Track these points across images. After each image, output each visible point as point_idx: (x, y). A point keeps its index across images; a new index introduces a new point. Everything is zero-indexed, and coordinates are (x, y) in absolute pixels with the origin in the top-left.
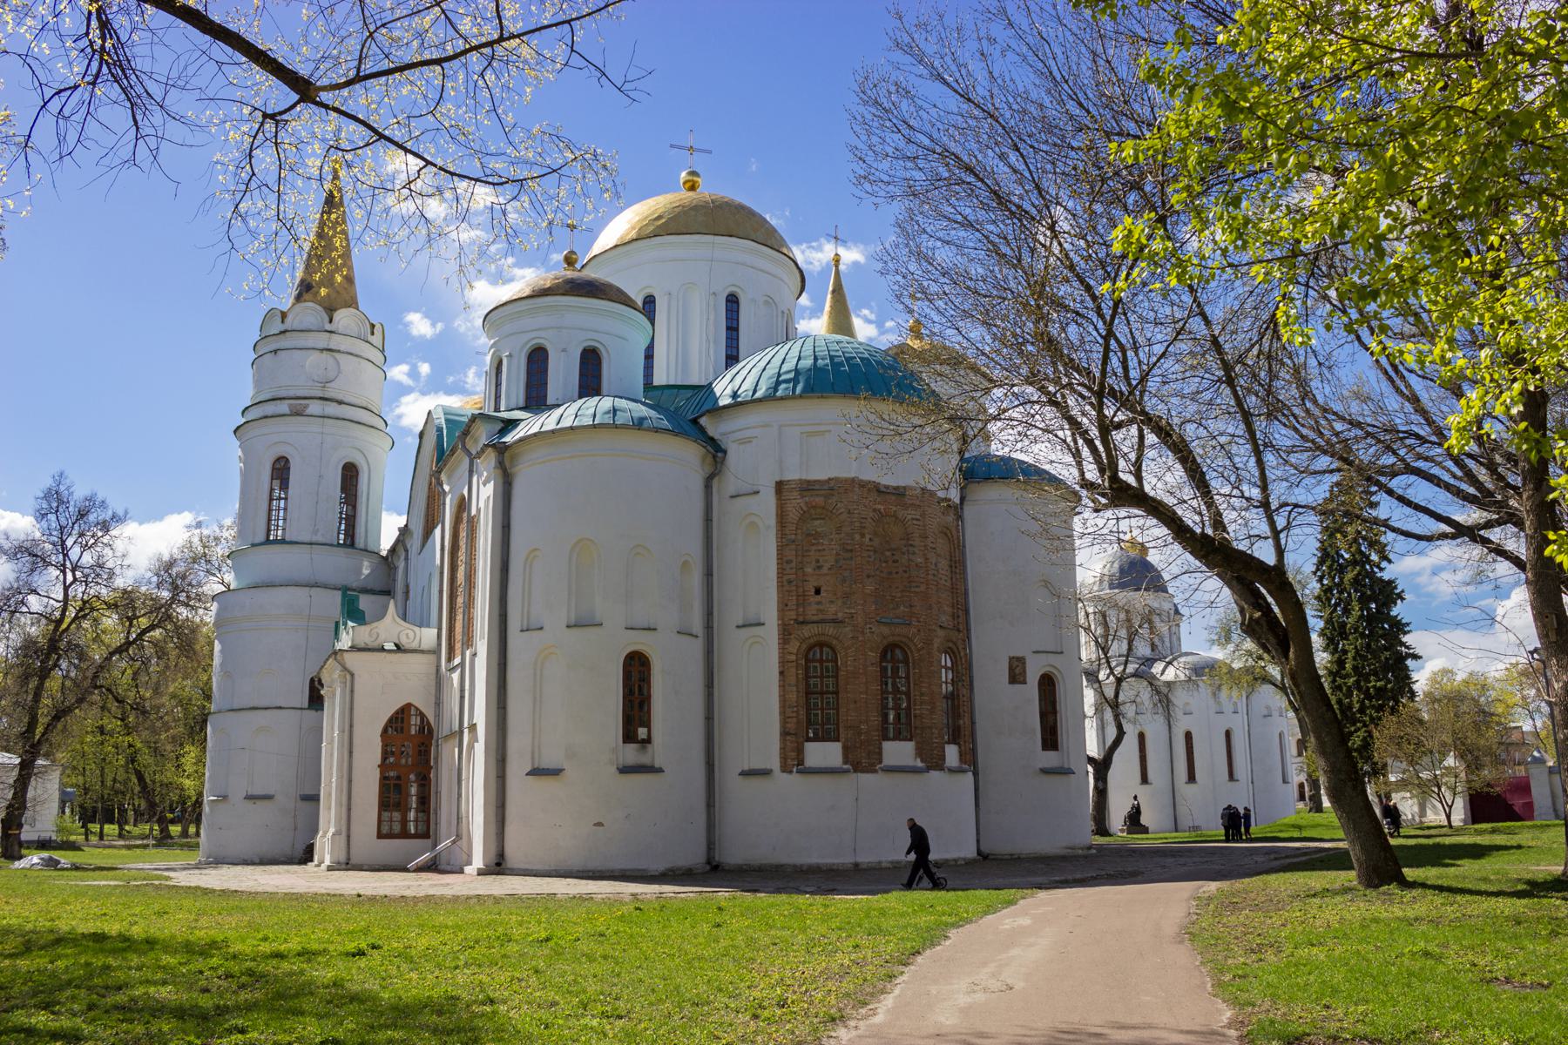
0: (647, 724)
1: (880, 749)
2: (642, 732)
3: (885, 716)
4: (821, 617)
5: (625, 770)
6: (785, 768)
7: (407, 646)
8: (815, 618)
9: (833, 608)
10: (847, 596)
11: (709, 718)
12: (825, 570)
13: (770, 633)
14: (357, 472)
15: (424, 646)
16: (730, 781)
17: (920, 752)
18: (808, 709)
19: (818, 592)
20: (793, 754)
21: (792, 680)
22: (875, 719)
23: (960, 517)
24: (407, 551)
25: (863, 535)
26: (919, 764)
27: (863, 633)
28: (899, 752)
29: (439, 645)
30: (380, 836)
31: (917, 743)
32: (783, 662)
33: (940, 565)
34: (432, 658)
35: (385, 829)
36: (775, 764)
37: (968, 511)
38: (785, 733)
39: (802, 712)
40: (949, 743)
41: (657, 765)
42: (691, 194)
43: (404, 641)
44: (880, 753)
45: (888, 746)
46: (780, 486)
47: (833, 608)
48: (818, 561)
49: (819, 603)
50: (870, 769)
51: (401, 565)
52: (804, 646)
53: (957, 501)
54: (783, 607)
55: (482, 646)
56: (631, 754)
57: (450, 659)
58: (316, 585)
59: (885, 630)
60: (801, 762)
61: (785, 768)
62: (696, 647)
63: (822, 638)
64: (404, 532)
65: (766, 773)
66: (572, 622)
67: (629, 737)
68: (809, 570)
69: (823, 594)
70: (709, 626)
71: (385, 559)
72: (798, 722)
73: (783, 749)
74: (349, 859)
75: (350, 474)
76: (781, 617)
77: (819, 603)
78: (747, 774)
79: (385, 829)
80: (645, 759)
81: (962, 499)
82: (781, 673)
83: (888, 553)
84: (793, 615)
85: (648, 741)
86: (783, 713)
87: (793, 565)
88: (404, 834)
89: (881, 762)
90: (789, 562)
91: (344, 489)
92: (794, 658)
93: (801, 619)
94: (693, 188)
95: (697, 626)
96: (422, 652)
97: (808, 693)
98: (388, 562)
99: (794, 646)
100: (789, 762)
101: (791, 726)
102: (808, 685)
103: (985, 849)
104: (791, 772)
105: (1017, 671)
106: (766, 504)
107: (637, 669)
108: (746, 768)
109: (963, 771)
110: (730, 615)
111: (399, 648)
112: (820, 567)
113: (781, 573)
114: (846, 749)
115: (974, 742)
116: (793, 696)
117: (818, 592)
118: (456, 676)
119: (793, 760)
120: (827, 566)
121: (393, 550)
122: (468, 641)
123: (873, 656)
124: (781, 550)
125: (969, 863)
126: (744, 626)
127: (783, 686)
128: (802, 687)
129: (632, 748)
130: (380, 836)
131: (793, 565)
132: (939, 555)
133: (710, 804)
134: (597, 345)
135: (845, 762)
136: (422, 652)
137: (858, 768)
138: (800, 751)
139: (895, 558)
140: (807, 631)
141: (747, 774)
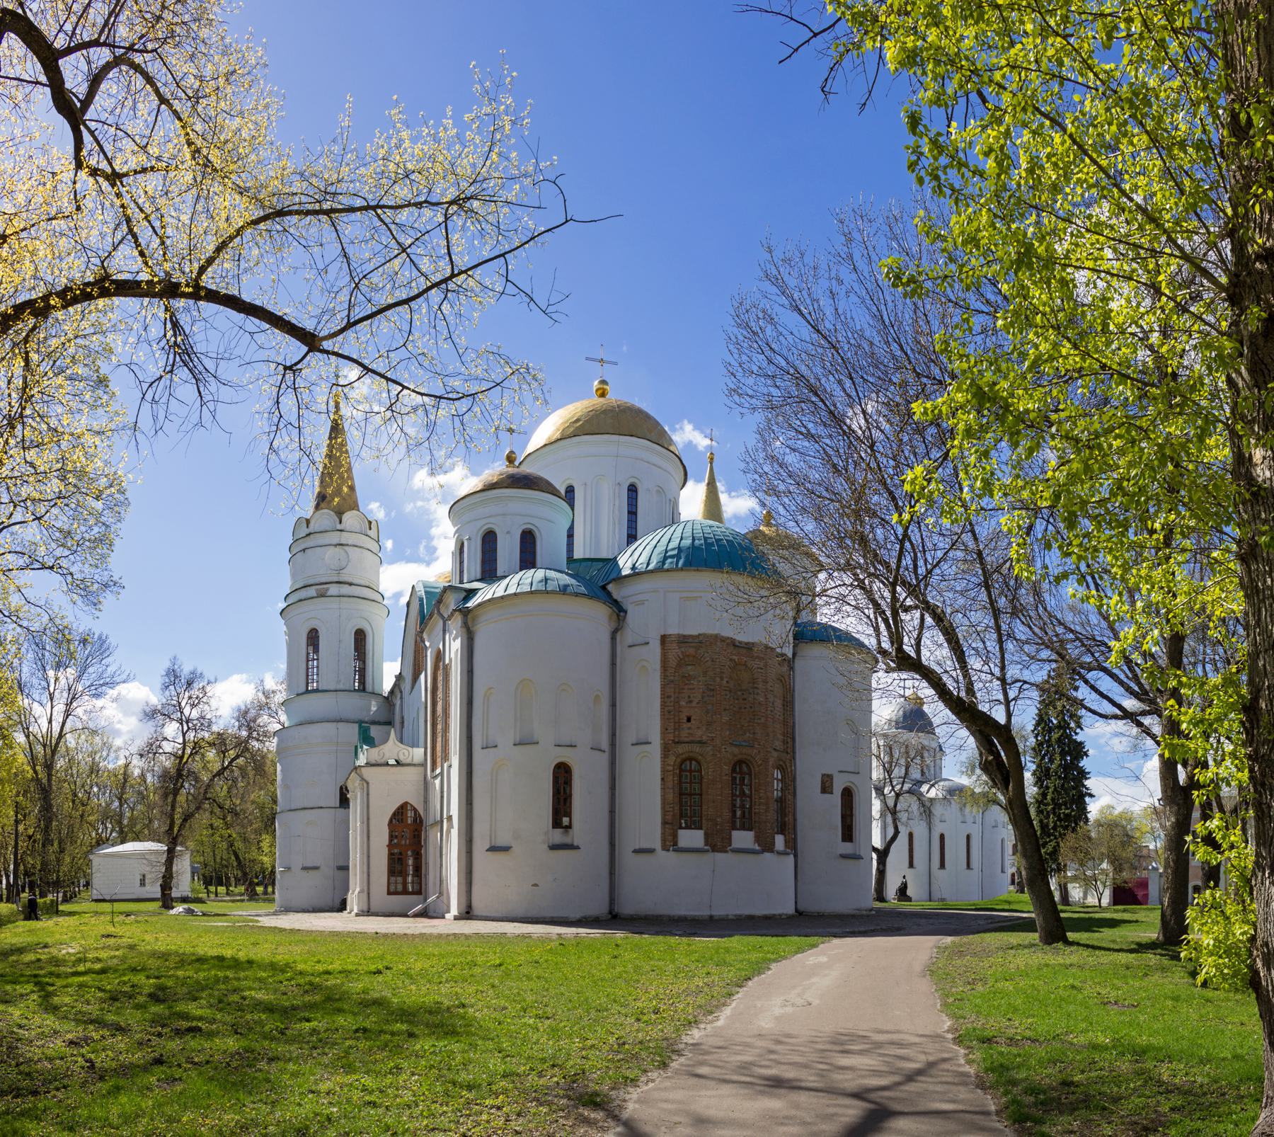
0: (569, 815)
1: (730, 836)
2: (565, 821)
3: (734, 812)
4: (691, 738)
5: (554, 847)
6: (665, 848)
7: (404, 762)
8: (687, 740)
9: (699, 733)
10: (709, 724)
11: (612, 812)
12: (694, 704)
13: (655, 749)
15: (415, 761)
18: (681, 806)
19: (689, 720)
20: (670, 838)
21: (670, 784)
22: (727, 814)
23: (792, 668)
24: (401, 692)
25: (722, 679)
26: (757, 848)
27: (720, 751)
28: (743, 838)
29: (426, 760)
32: (664, 771)
33: (776, 704)
34: (421, 769)
36: (657, 844)
37: (798, 664)
38: (664, 823)
39: (677, 808)
40: (778, 833)
41: (575, 844)
43: (402, 758)
44: (730, 839)
45: (735, 834)
47: (699, 733)
49: (689, 728)
50: (723, 850)
51: (398, 703)
52: (679, 760)
53: (790, 655)
54: (664, 731)
55: (455, 760)
56: (558, 836)
57: (433, 770)
59: (736, 750)
60: (675, 844)
61: (665, 848)
62: (604, 759)
63: (691, 754)
64: (399, 678)
65: (650, 851)
66: (517, 742)
67: (557, 824)
68: (683, 703)
69: (693, 722)
70: (613, 744)
71: (386, 698)
72: (674, 815)
73: (663, 834)
75: (360, 638)
76: (663, 738)
77: (689, 728)
78: (638, 851)
80: (567, 840)
81: (794, 655)
82: (663, 779)
83: (739, 693)
84: (671, 736)
85: (569, 827)
86: (663, 808)
91: (356, 649)
92: (671, 768)
95: (605, 745)
96: (414, 765)
97: (681, 794)
98: (389, 701)
99: (672, 759)
100: (668, 843)
101: (669, 818)
102: (681, 788)
103: (801, 908)
104: (668, 850)
107: (562, 775)
108: (637, 847)
109: (788, 854)
110: (628, 735)
112: (691, 702)
114: (707, 836)
115: (795, 833)
116: (670, 796)
117: (689, 720)
118: (437, 782)
119: (670, 842)
120: (696, 700)
121: (392, 692)
122: (446, 757)
123: (727, 769)
125: (789, 918)
126: (637, 744)
127: (663, 789)
128: (677, 790)
129: (559, 831)
132: (775, 696)
133: (612, 873)
135: (706, 845)
136: (414, 765)
137: (714, 849)
138: (675, 836)
139: (745, 697)
140: (681, 749)
141: (638, 851)
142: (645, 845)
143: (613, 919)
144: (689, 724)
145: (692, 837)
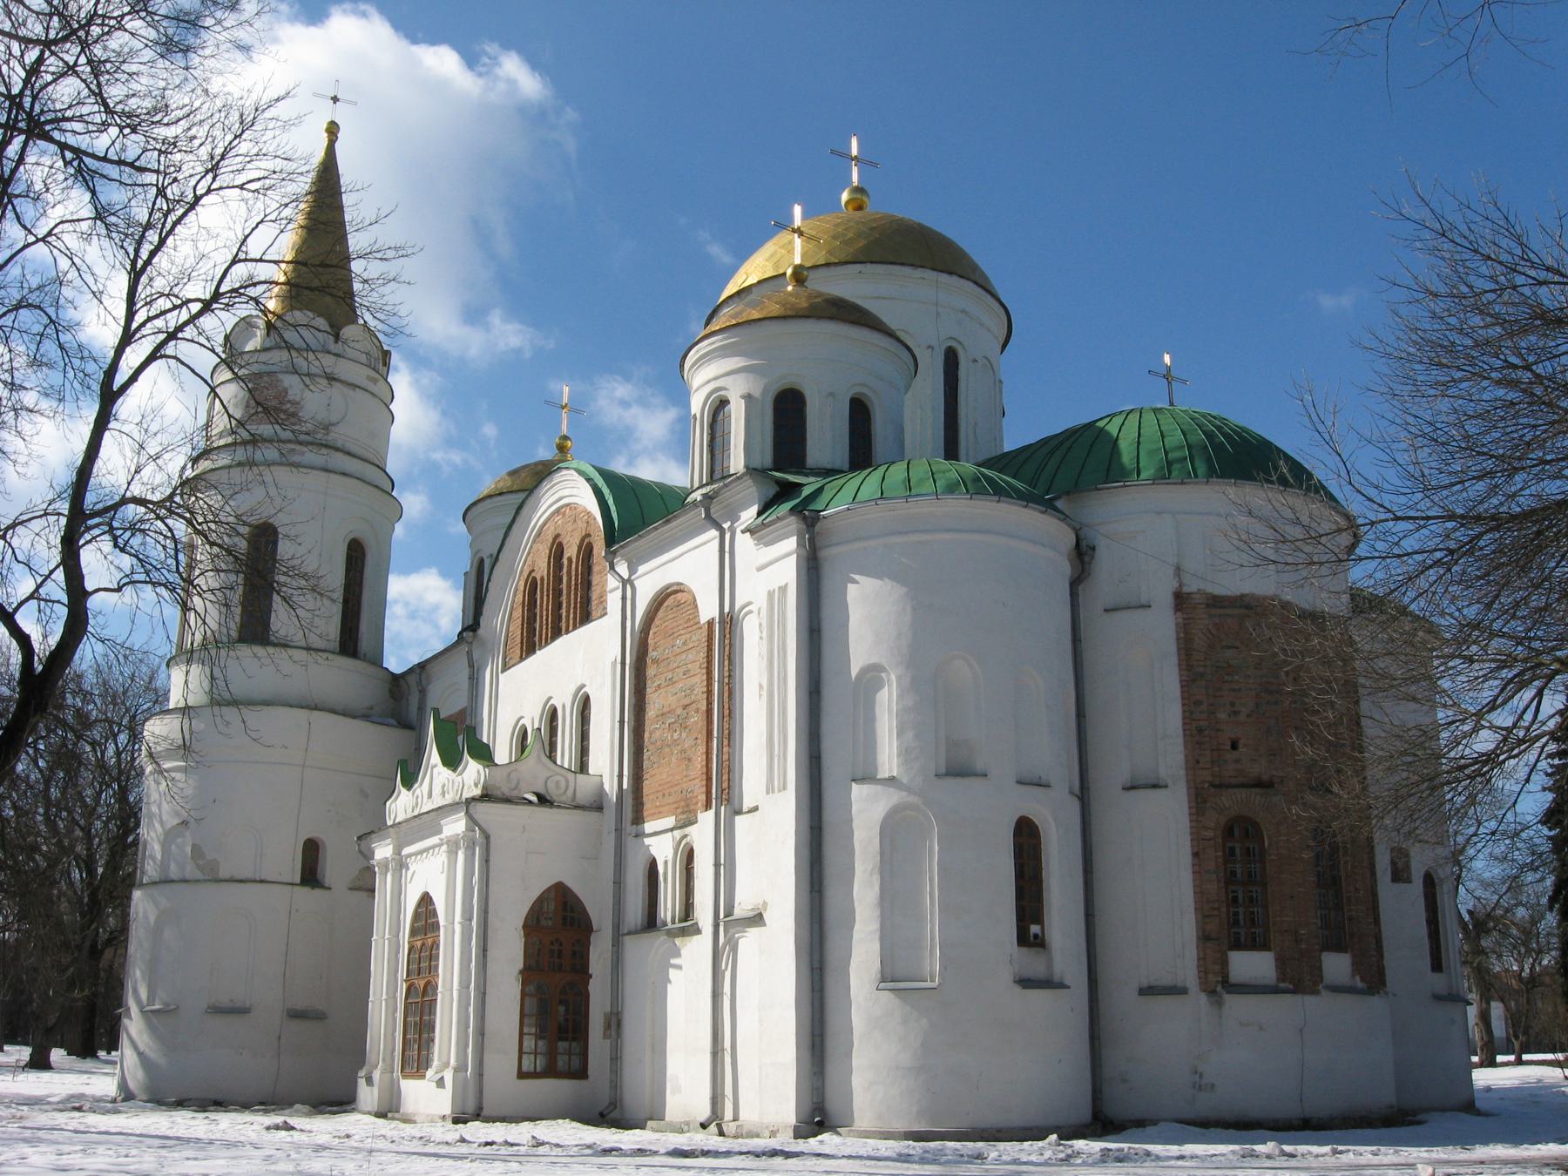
5: (1025, 983)
12: (1242, 717)
14: (364, 554)
16: (1122, 998)
17: (1357, 966)
19: (1234, 746)
20: (1217, 968)
30: (522, 1075)
31: (1354, 956)
35: (527, 1064)
38: (1204, 938)
42: (859, 213)
43: (553, 793)
46: (1181, 600)
48: (1233, 704)
54: (1192, 764)
58: (316, 708)
67: (1024, 939)
68: (1222, 716)
69: (1242, 749)
73: (1202, 958)
74: (481, 1108)
77: (1237, 761)
78: (1148, 991)
79: (527, 1064)
82: (1195, 855)
87: (1204, 707)
88: (550, 1071)
89: (1322, 982)
90: (1198, 703)
92: (1210, 834)
93: (1217, 782)
94: (860, 208)
100: (1211, 976)
105: (1400, 865)
106: (1161, 627)
108: (1145, 983)
110: (1113, 769)
111: (543, 800)
112: (1236, 713)
113: (1188, 718)
114: (1281, 962)
117: (1234, 746)
124: (1186, 686)
126: (1133, 788)
130: (522, 1075)
131: (1204, 707)
134: (869, 393)
138: (1224, 963)
142: (1166, 980)
143: (1102, 1124)
144: (1235, 754)
145: (1252, 965)
